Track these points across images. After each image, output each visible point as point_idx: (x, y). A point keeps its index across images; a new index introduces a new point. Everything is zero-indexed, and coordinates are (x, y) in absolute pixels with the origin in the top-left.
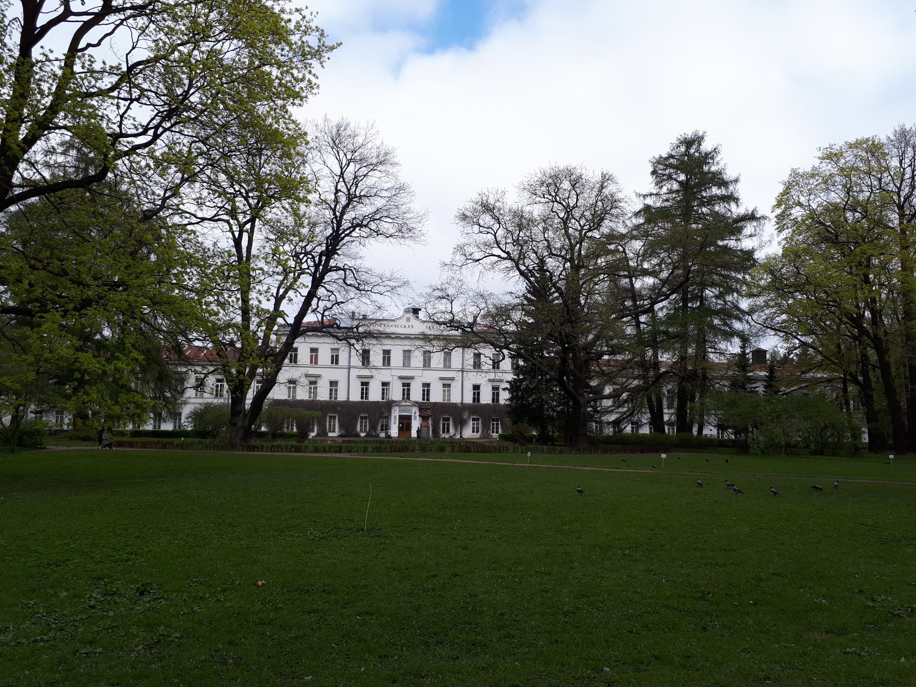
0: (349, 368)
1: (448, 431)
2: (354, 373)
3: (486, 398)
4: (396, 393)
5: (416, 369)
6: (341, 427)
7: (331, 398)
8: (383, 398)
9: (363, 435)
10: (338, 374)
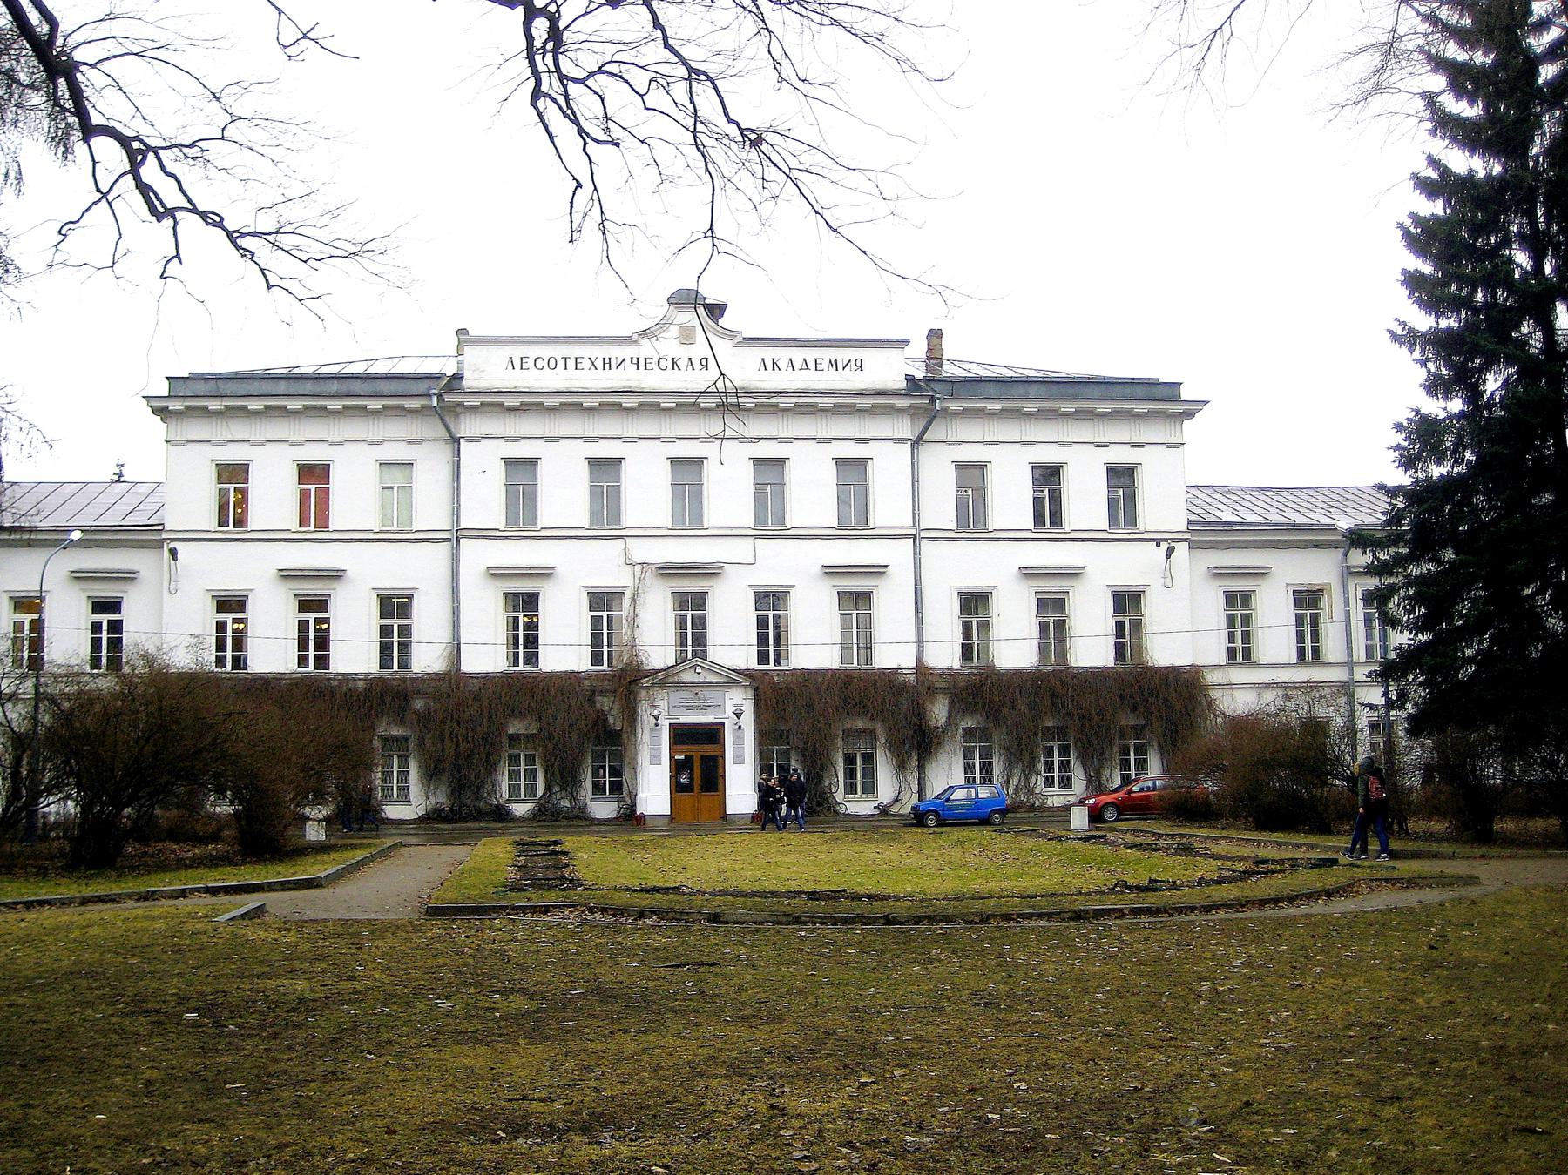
0: (456, 536)
1: (870, 789)
2: (478, 557)
4: (655, 640)
5: (729, 533)
6: (431, 774)
7: (385, 663)
8: (596, 658)
9: (521, 809)
10: (415, 569)
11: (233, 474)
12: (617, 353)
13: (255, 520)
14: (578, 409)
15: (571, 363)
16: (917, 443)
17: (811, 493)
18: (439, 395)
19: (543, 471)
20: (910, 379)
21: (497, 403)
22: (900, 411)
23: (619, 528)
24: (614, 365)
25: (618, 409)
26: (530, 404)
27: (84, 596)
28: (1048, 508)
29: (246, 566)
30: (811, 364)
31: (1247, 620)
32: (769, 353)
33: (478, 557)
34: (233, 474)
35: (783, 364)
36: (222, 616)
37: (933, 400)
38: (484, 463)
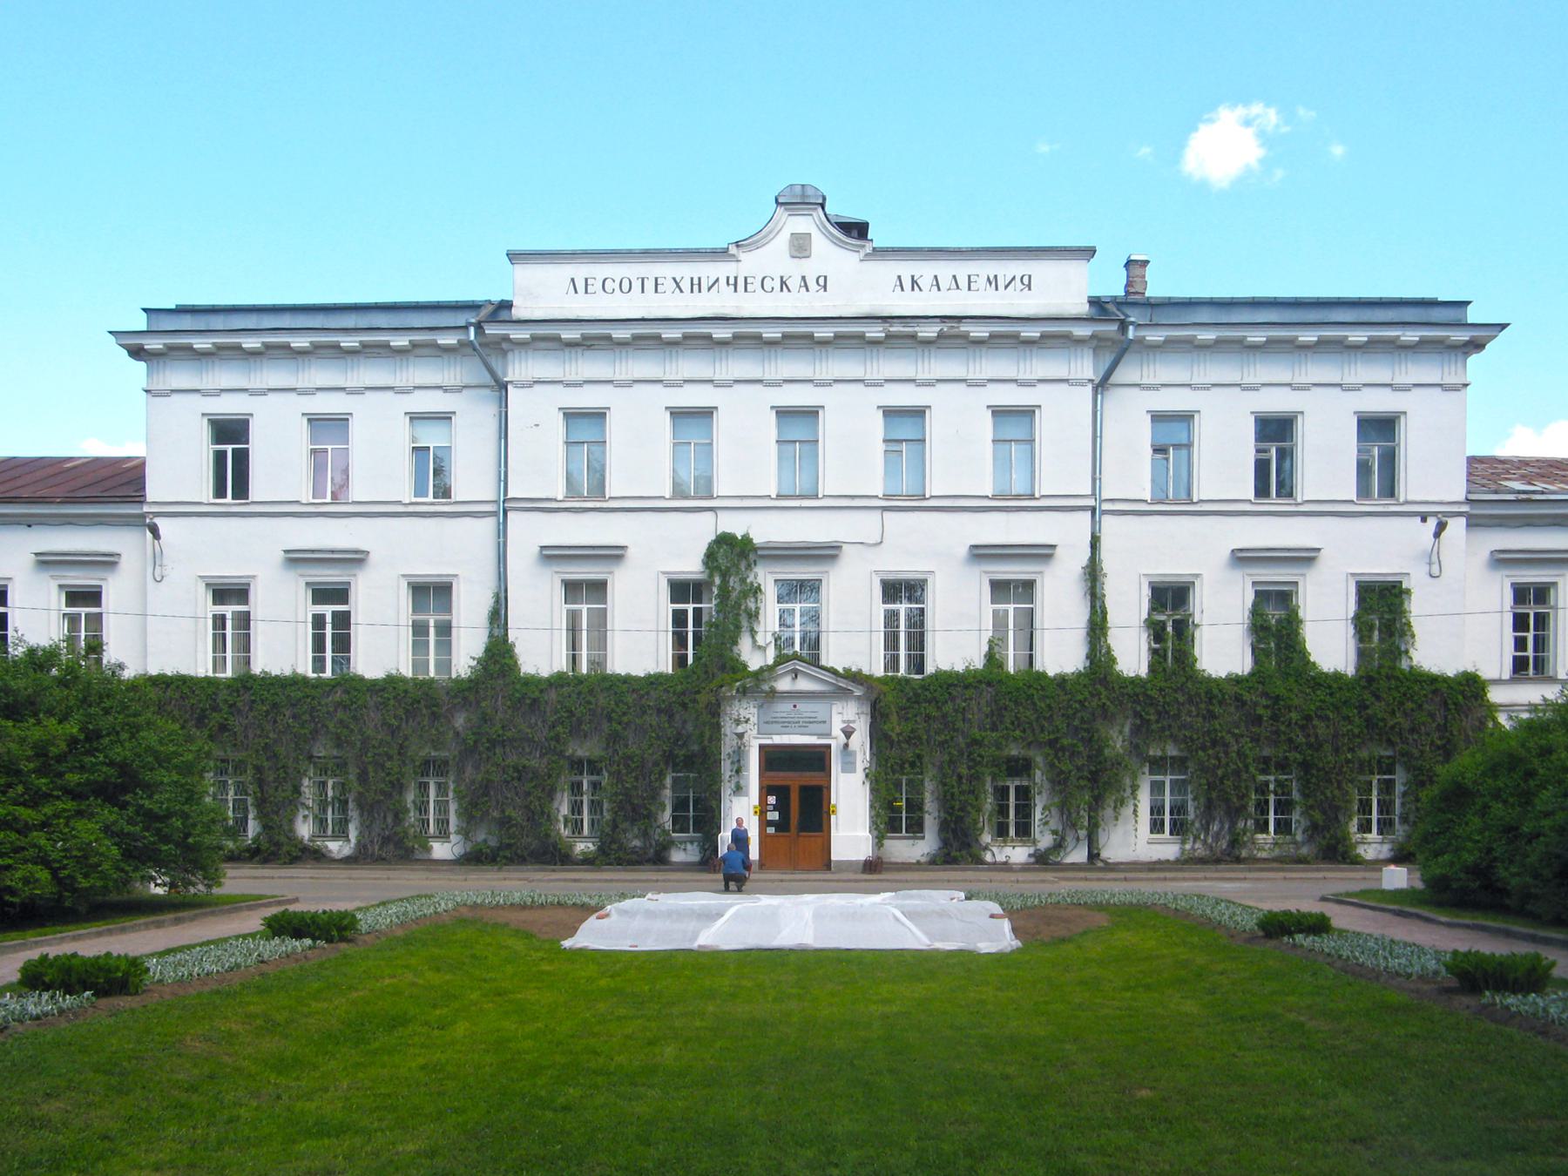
0: (503, 509)
2: (528, 533)
3: (1223, 651)
5: (851, 504)
11: (230, 431)
12: (708, 271)
13: (259, 488)
14: (657, 343)
15: (650, 285)
16: (1102, 385)
17: (961, 450)
18: (479, 327)
19: (612, 421)
20: (1095, 302)
21: (553, 338)
22: (1080, 342)
23: (711, 497)
24: (704, 286)
25: (708, 342)
26: (594, 338)
27: (54, 585)
28: (1274, 471)
29: (247, 547)
30: (963, 283)
31: (1542, 621)
32: (907, 269)
33: (528, 533)
34: (230, 431)
35: (925, 282)
36: (220, 609)
37: (1124, 326)
38: (537, 410)
